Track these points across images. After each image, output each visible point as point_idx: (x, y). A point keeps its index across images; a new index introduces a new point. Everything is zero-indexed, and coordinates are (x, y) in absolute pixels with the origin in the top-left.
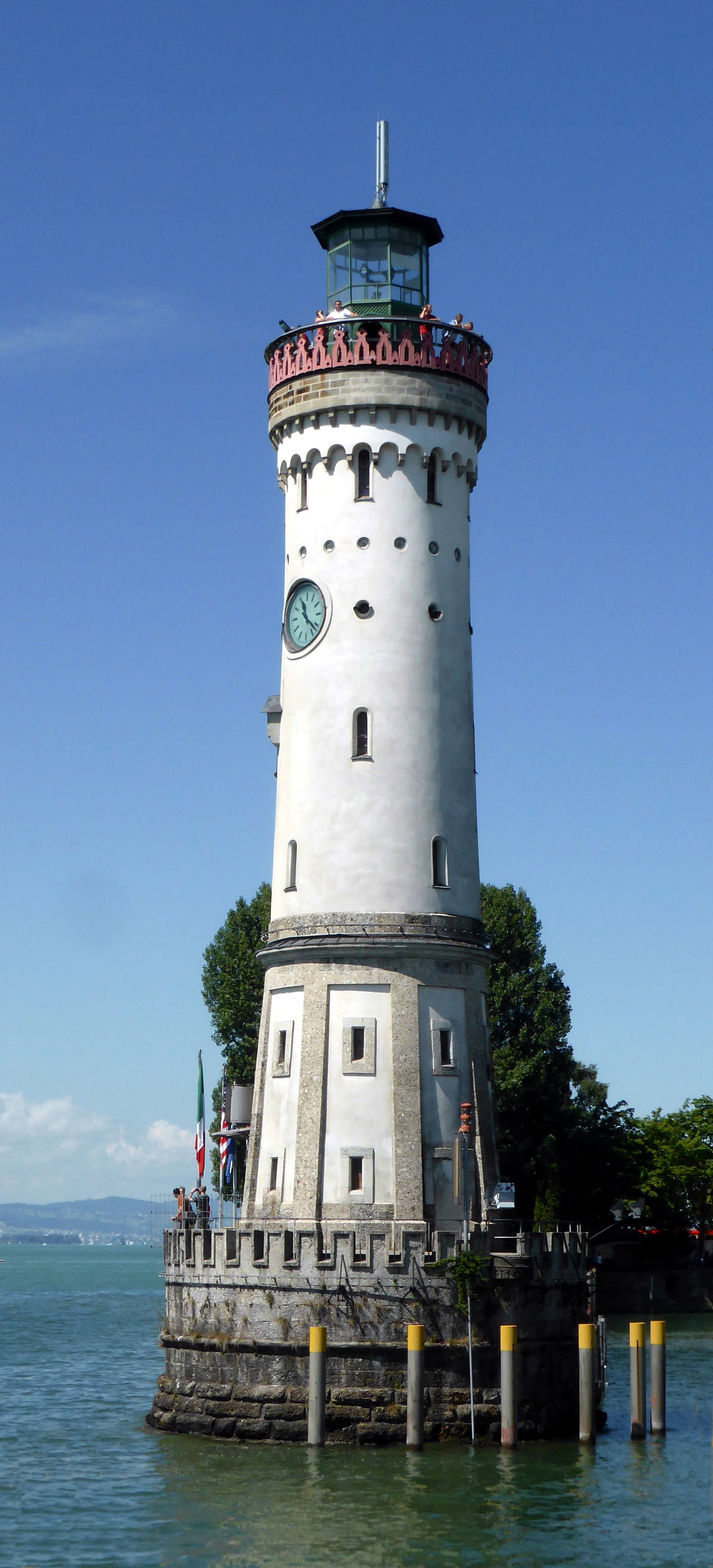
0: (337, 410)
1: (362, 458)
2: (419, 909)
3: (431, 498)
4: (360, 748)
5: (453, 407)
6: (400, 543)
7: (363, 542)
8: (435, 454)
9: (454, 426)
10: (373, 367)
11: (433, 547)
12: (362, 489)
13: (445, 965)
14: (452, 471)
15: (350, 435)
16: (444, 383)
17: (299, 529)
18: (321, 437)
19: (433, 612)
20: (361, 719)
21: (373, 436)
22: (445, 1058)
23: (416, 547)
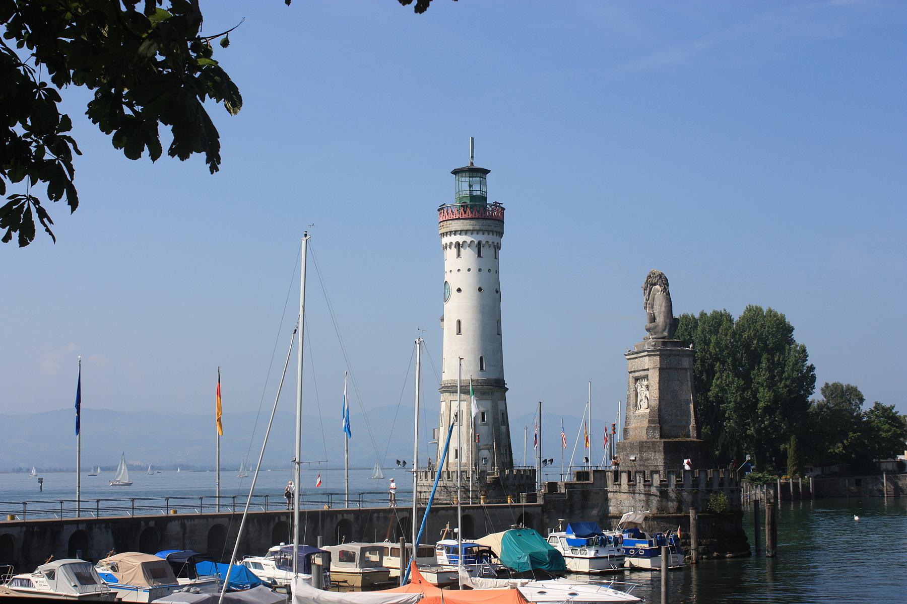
0: (451, 232)
1: (458, 245)
2: (474, 378)
3: (479, 255)
4: (459, 332)
5: (484, 228)
6: (469, 270)
7: (459, 270)
8: (479, 243)
9: (486, 233)
10: (459, 219)
11: (480, 270)
12: (459, 255)
13: (483, 393)
14: (487, 246)
15: (454, 239)
16: (481, 221)
17: (448, 265)
18: (446, 240)
19: (480, 289)
20: (459, 322)
21: (460, 238)
22: (483, 419)
23: (474, 270)
